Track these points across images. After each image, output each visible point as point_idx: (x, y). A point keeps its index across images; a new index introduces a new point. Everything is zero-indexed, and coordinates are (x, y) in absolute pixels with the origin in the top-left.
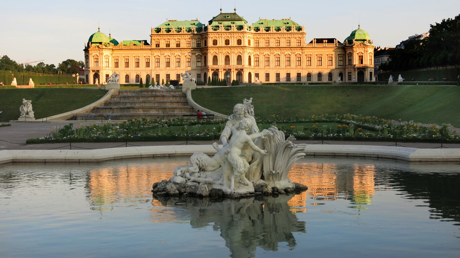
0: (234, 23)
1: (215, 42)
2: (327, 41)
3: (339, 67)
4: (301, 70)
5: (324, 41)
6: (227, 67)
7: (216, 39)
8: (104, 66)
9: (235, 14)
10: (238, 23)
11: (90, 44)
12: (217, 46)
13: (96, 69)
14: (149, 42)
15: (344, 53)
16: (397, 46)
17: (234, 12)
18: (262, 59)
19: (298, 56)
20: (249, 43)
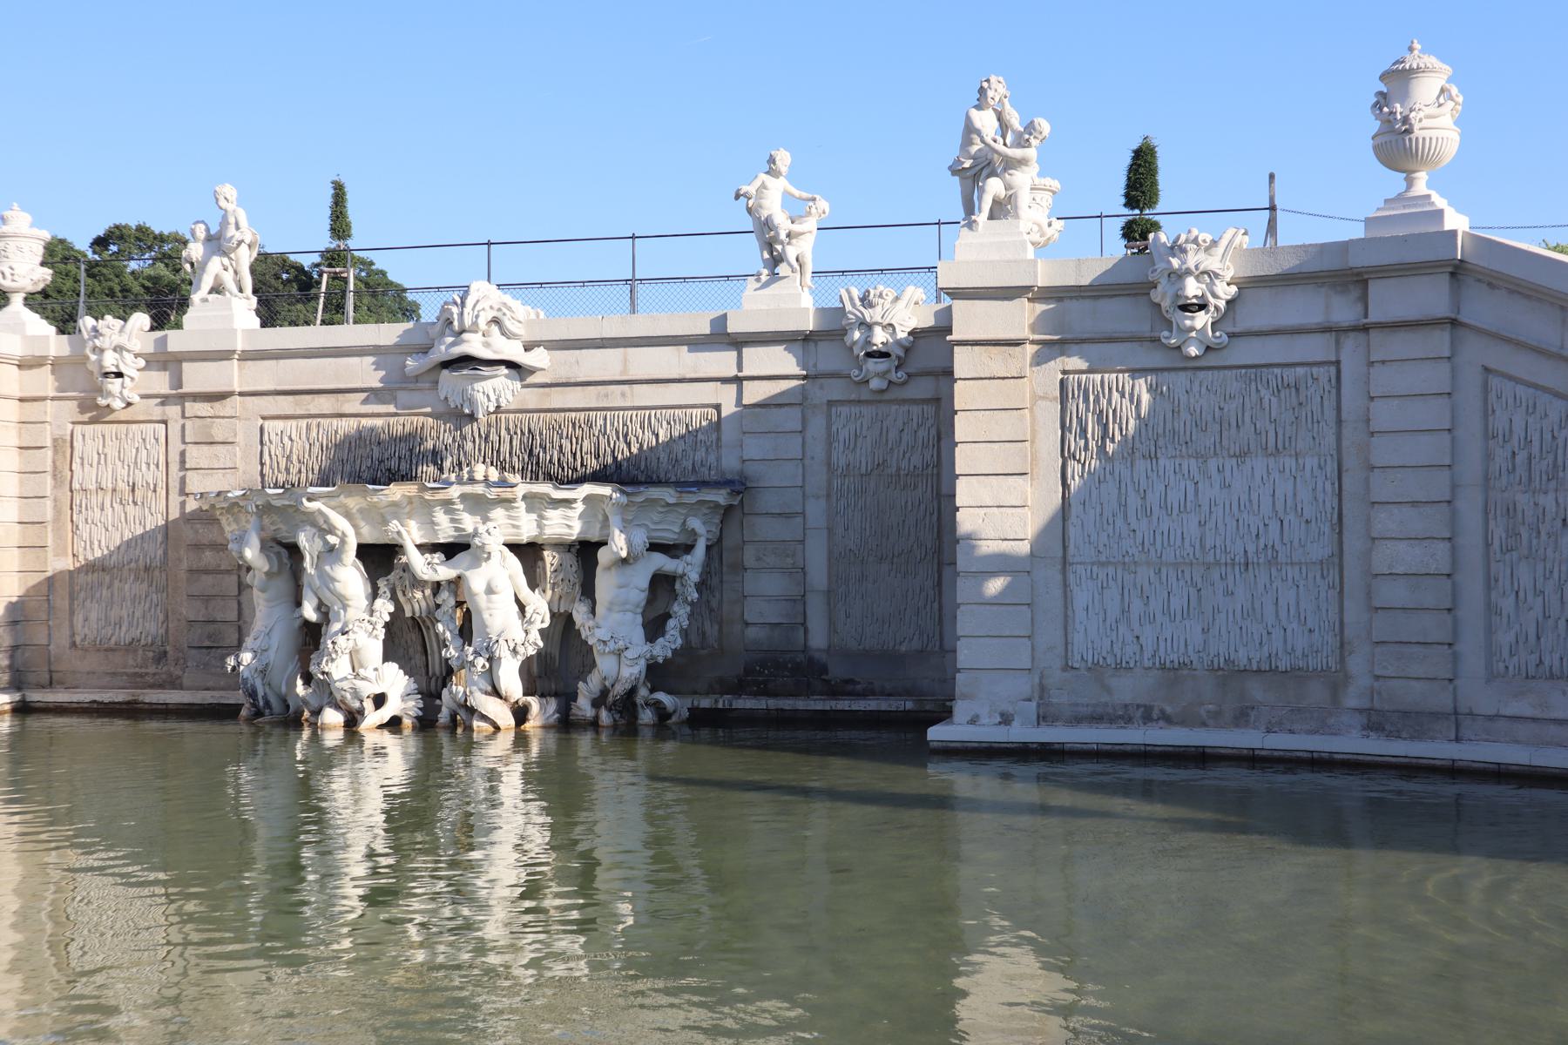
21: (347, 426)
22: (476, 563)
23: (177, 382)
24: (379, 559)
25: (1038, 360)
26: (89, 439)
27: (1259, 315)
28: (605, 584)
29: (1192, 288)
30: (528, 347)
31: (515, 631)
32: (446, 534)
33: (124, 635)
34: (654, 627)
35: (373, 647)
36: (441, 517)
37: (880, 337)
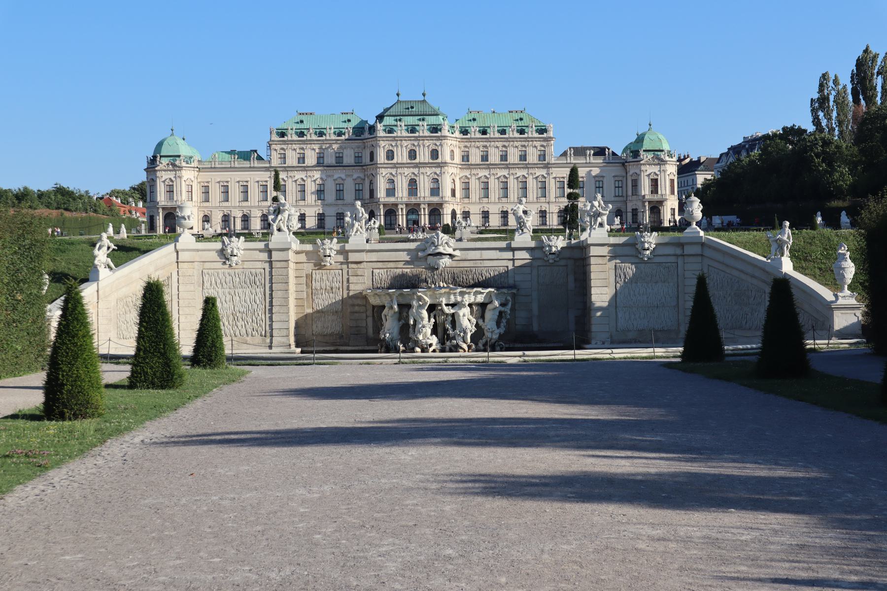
0: (423, 120)
1: (390, 155)
2: (592, 152)
3: (617, 199)
4: (547, 206)
5: (588, 152)
6: (413, 200)
7: (391, 148)
8: (184, 198)
9: (424, 101)
10: (432, 120)
11: (158, 159)
12: (395, 161)
13: (169, 204)
14: (263, 153)
15: (624, 174)
16: (721, 155)
17: (422, 98)
18: (475, 186)
19: (540, 179)
20: (452, 158)
21: (399, 271)
22: (460, 309)
23: (347, 258)
24: (432, 308)
25: (610, 260)
26: (317, 274)
27: (661, 251)
28: (488, 315)
29: (646, 246)
30: (454, 250)
31: (469, 326)
32: (452, 300)
33: (329, 331)
34: (498, 324)
35: (429, 331)
36: (452, 297)
37: (554, 249)
